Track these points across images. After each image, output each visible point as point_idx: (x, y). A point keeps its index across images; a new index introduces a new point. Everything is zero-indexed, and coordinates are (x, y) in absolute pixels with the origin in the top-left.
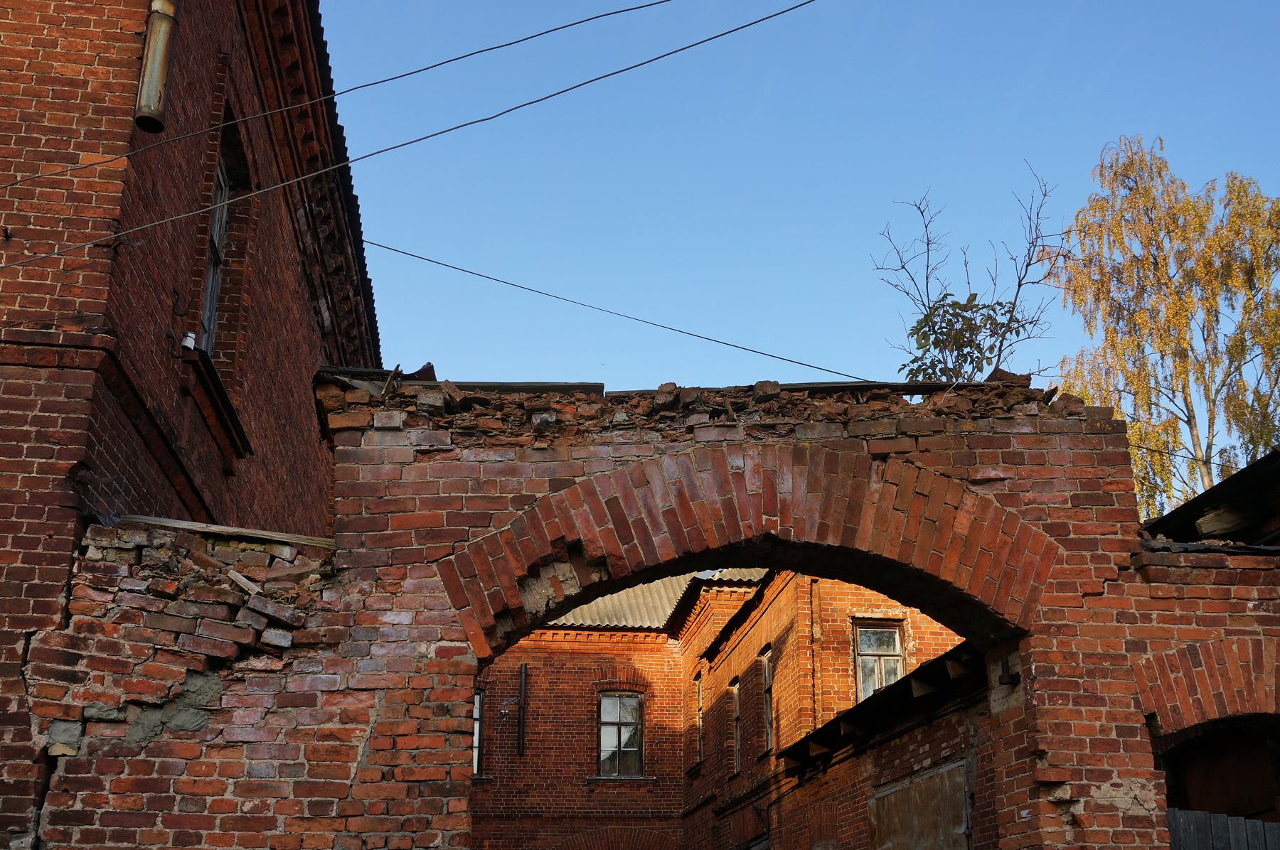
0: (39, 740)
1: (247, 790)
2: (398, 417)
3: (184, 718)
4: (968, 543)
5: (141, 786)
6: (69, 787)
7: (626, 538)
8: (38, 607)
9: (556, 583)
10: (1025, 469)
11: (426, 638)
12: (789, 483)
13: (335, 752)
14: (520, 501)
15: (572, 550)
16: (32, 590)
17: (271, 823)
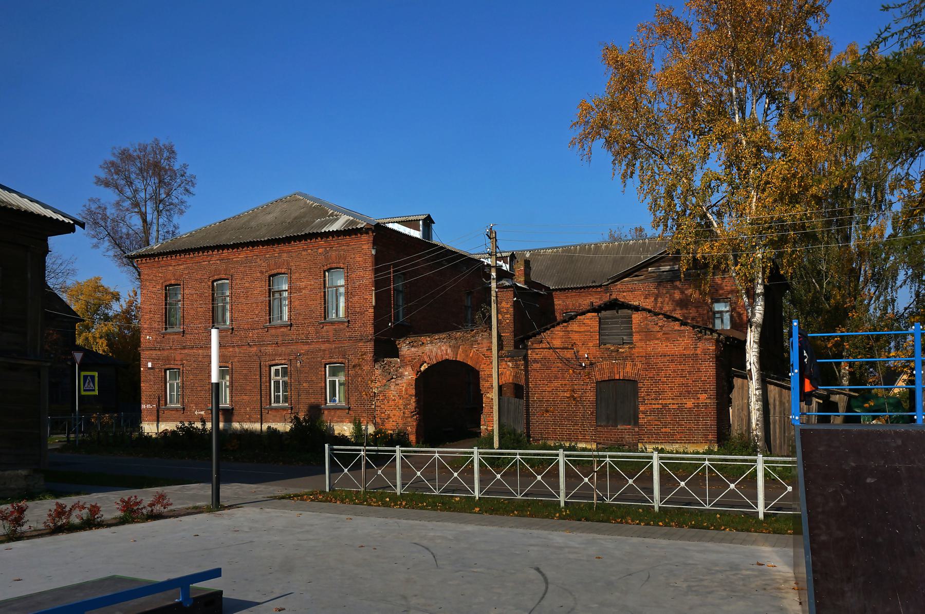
0: (374, 391)
1: (393, 396)
2: (405, 345)
3: (387, 387)
4: (471, 358)
5: (384, 396)
6: (377, 396)
7: (430, 360)
8: (372, 374)
9: (425, 367)
10: (480, 345)
11: (410, 376)
12: (449, 351)
13: (401, 391)
14: (419, 356)
15: (425, 362)
16: (371, 372)
17: (396, 400)
